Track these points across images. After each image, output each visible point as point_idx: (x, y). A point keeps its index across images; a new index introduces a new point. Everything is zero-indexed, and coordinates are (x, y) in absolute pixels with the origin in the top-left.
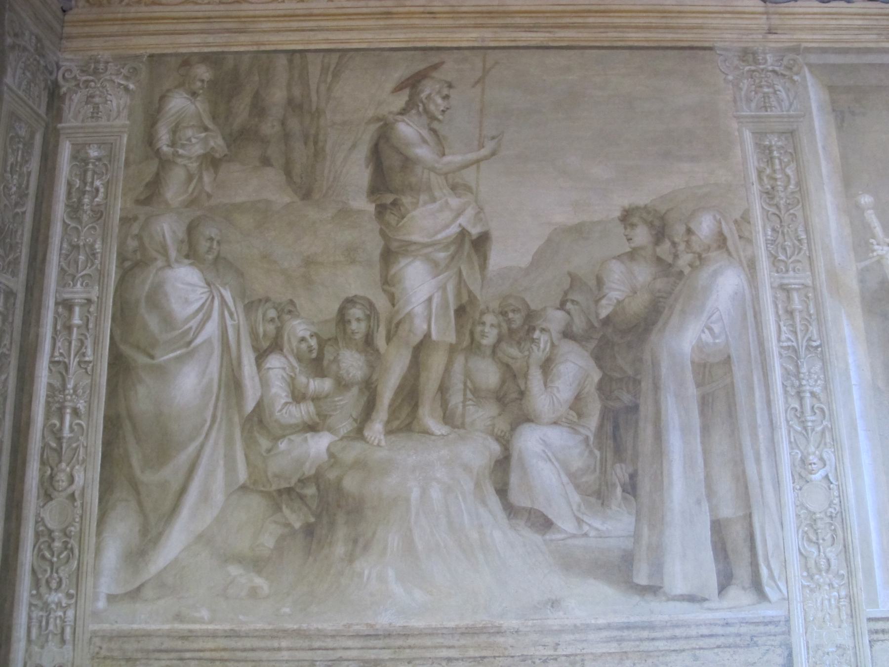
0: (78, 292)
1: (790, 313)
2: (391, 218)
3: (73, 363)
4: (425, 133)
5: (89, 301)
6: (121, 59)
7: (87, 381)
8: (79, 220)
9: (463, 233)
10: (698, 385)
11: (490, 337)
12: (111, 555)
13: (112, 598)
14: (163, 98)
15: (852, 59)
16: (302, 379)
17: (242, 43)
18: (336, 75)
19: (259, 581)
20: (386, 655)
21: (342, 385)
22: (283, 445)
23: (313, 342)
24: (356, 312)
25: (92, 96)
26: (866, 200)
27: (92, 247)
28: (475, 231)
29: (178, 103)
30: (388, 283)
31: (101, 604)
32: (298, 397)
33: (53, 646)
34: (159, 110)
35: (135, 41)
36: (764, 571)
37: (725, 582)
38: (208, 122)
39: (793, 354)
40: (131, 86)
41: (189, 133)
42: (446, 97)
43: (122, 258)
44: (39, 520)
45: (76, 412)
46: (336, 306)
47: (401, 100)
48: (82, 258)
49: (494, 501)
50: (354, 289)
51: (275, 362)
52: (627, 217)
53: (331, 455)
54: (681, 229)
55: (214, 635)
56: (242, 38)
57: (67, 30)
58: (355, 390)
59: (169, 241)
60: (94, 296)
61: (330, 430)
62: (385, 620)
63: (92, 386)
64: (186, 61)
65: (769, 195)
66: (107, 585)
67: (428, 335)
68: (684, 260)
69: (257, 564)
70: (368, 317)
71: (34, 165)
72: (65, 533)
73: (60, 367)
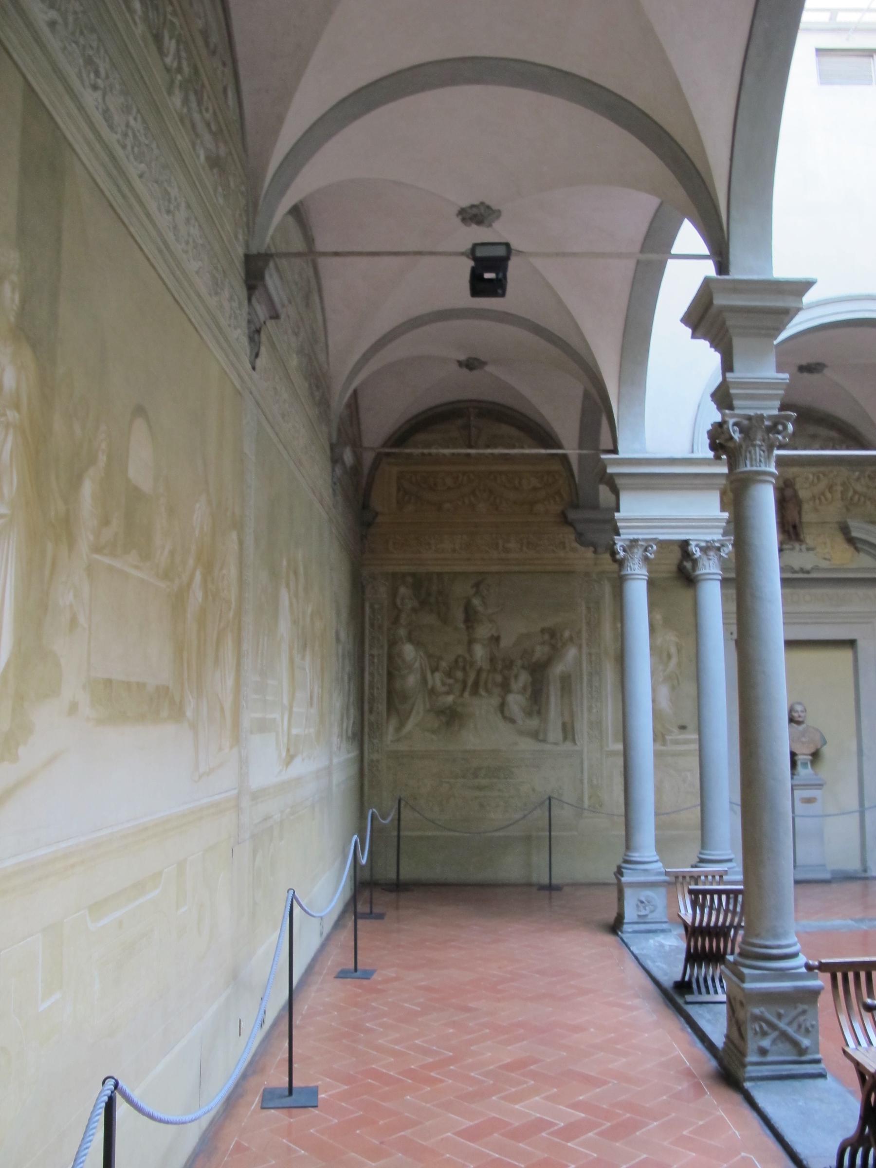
0: (375, 652)
1: (591, 661)
11: (500, 666)
12: (391, 729)
13: (392, 741)
19: (434, 737)
24: (460, 660)
28: (496, 634)
29: (403, 590)
30: (470, 650)
32: (444, 684)
37: (565, 738)
39: (590, 674)
40: (387, 583)
45: (378, 688)
49: (500, 715)
51: (438, 675)
52: (543, 631)
53: (454, 702)
64: (404, 575)
65: (588, 624)
69: (433, 732)
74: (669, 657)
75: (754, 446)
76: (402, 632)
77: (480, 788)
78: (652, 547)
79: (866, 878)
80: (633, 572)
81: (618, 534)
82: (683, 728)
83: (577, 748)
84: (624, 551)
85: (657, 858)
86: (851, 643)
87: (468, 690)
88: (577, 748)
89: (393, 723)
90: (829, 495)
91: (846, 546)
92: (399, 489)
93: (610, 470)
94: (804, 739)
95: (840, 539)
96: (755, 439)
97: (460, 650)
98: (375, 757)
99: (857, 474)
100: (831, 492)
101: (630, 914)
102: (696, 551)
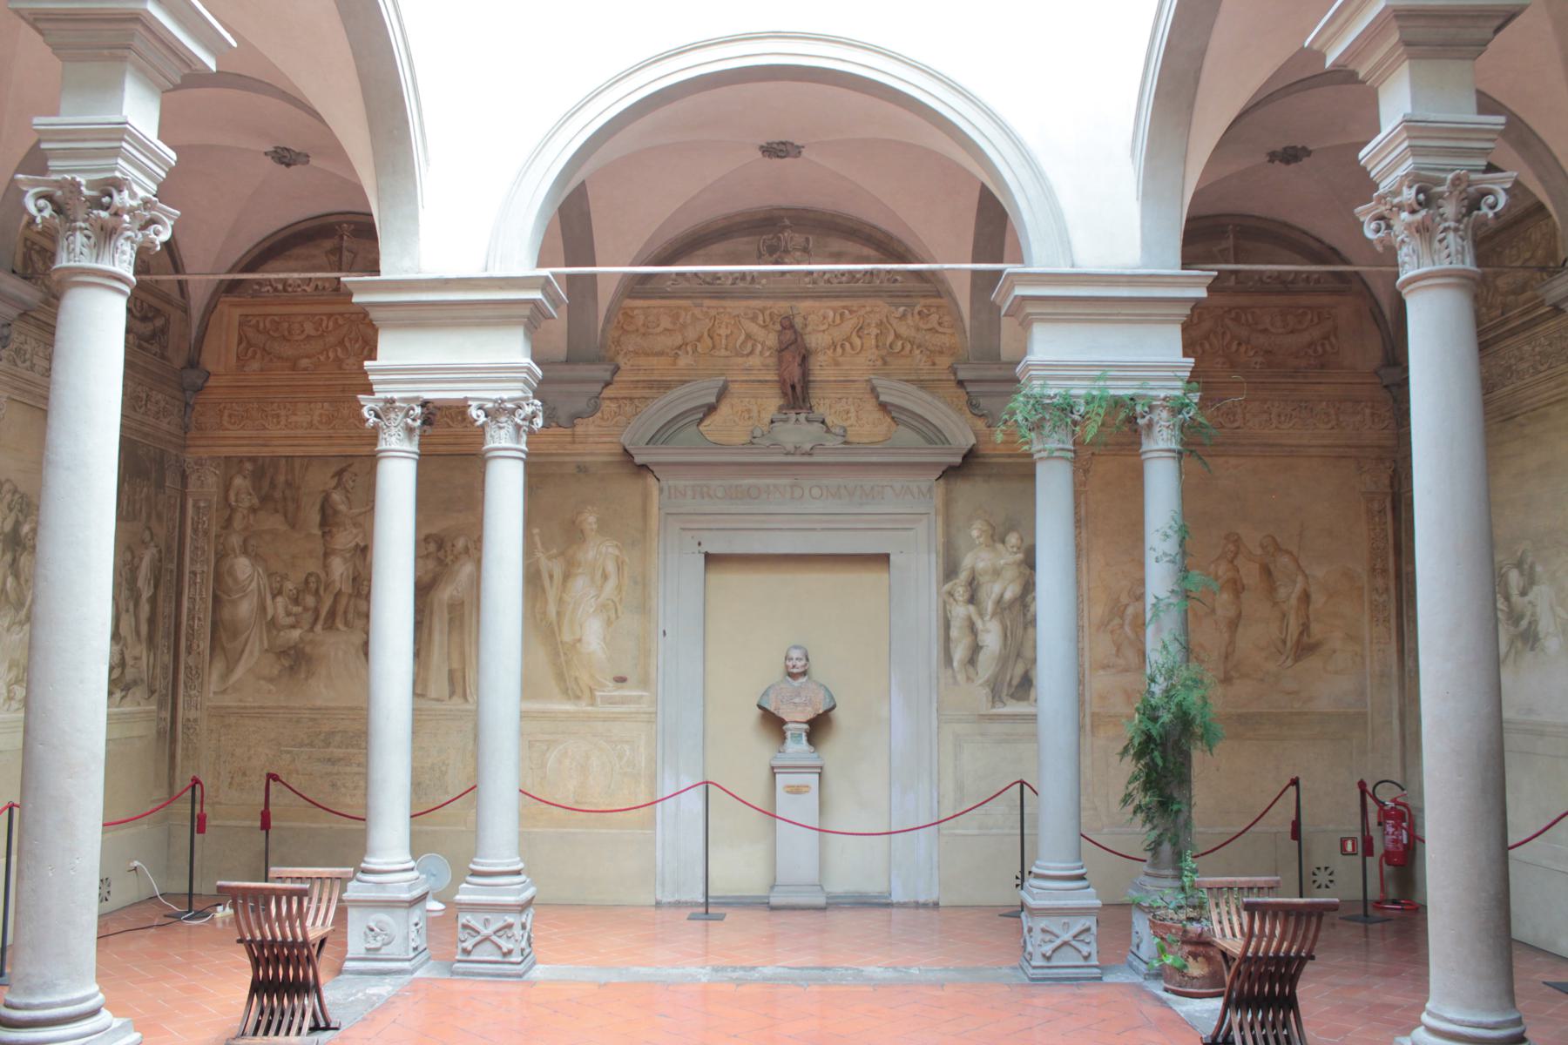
2: (328, 538)
3: (198, 599)
4: (344, 499)
5: (203, 572)
6: (213, 458)
7: (203, 606)
8: (197, 535)
9: (357, 545)
10: (449, 613)
12: (215, 676)
13: (215, 693)
14: (231, 478)
15: (543, 459)
16: (290, 607)
17: (265, 452)
18: (307, 468)
19: (272, 687)
20: (319, 716)
21: (306, 609)
22: (282, 633)
23: (295, 591)
24: (312, 579)
25: (200, 477)
26: (536, 531)
27: (203, 548)
28: (362, 544)
29: (238, 481)
30: (326, 567)
31: (211, 695)
32: (289, 614)
33: (193, 711)
34: (230, 483)
35: (216, 449)
36: (468, 691)
37: (452, 694)
38: (251, 491)
40: (217, 472)
41: (243, 496)
42: (354, 481)
43: (216, 553)
44: (186, 663)
45: (199, 619)
46: (304, 576)
47: (334, 483)
48: (199, 553)
50: (313, 569)
51: (279, 599)
53: (301, 638)
54: (449, 544)
55: (254, 708)
56: (266, 449)
57: (188, 442)
58: (310, 612)
59: (236, 546)
60: (205, 569)
61: (301, 628)
62: (319, 703)
63: (206, 608)
64: (241, 460)
66: (213, 688)
67: (340, 589)
68: (450, 558)
69: (271, 680)
70: (317, 582)
71: (177, 514)
72: (197, 667)
73: (192, 600)
74: (605, 577)
75: (74, 230)
76: (235, 540)
77: (332, 761)
78: (413, 410)
79: (889, 905)
80: (388, 447)
81: (372, 393)
82: (621, 680)
83: (468, 707)
84: (377, 416)
85: (412, 864)
86: (883, 559)
87: (321, 622)
88: (468, 707)
89: (219, 666)
90: (857, 342)
91: (878, 415)
92: (240, 342)
93: (355, 299)
94: (797, 700)
95: (870, 406)
96: (75, 221)
97: (313, 566)
98: (192, 714)
99: (902, 309)
100: (860, 337)
101: (356, 943)
102: (478, 416)
